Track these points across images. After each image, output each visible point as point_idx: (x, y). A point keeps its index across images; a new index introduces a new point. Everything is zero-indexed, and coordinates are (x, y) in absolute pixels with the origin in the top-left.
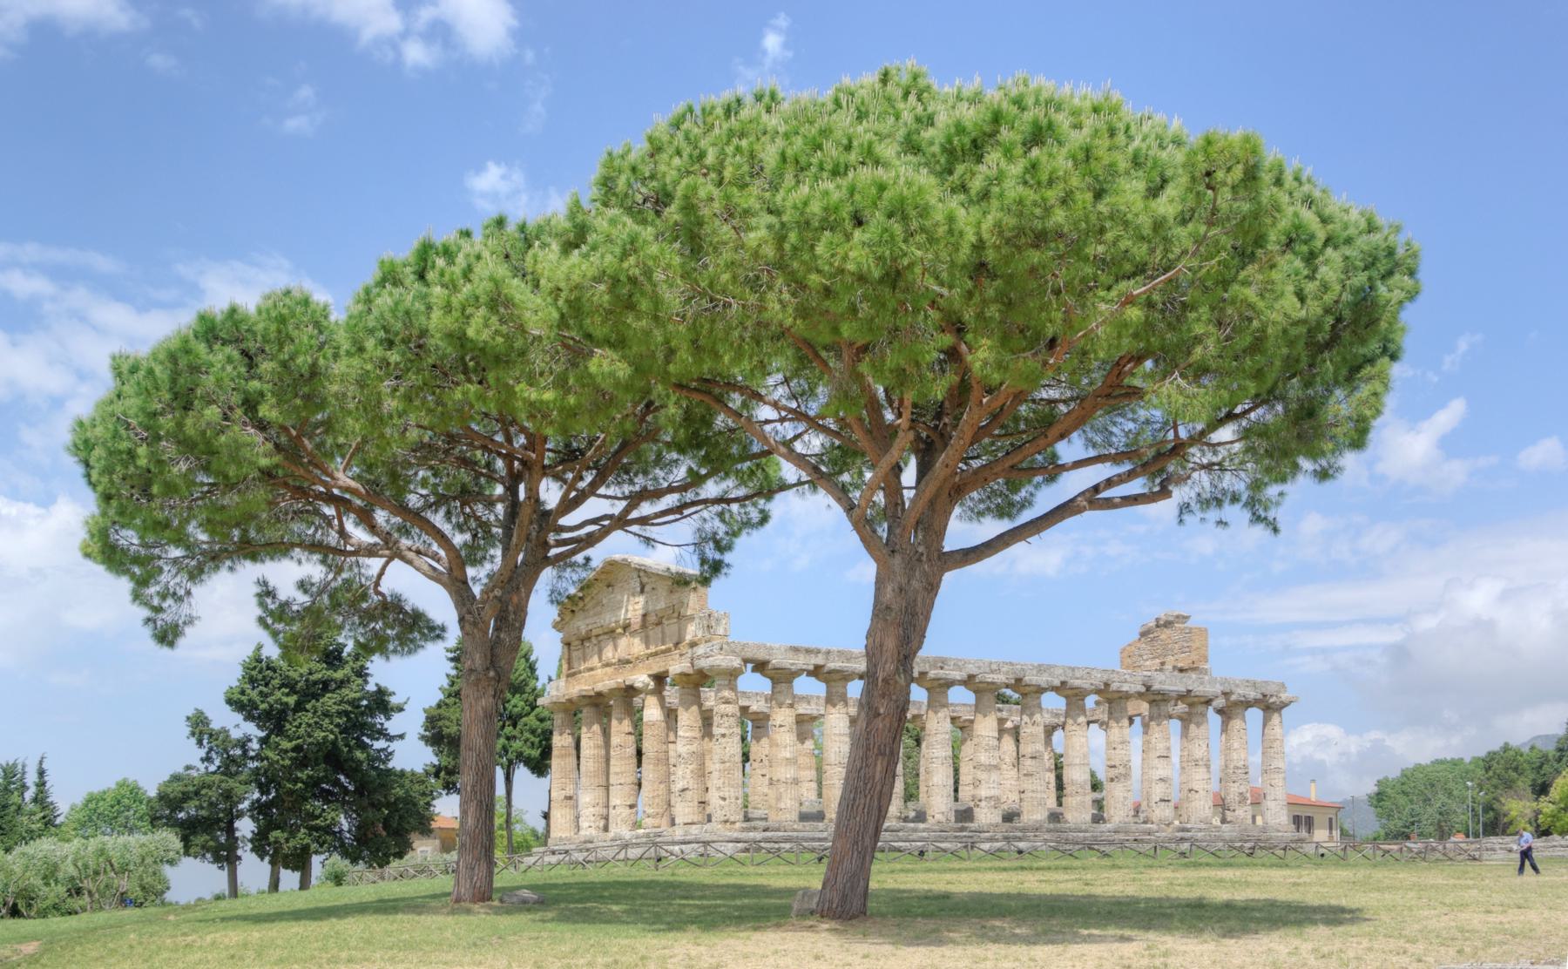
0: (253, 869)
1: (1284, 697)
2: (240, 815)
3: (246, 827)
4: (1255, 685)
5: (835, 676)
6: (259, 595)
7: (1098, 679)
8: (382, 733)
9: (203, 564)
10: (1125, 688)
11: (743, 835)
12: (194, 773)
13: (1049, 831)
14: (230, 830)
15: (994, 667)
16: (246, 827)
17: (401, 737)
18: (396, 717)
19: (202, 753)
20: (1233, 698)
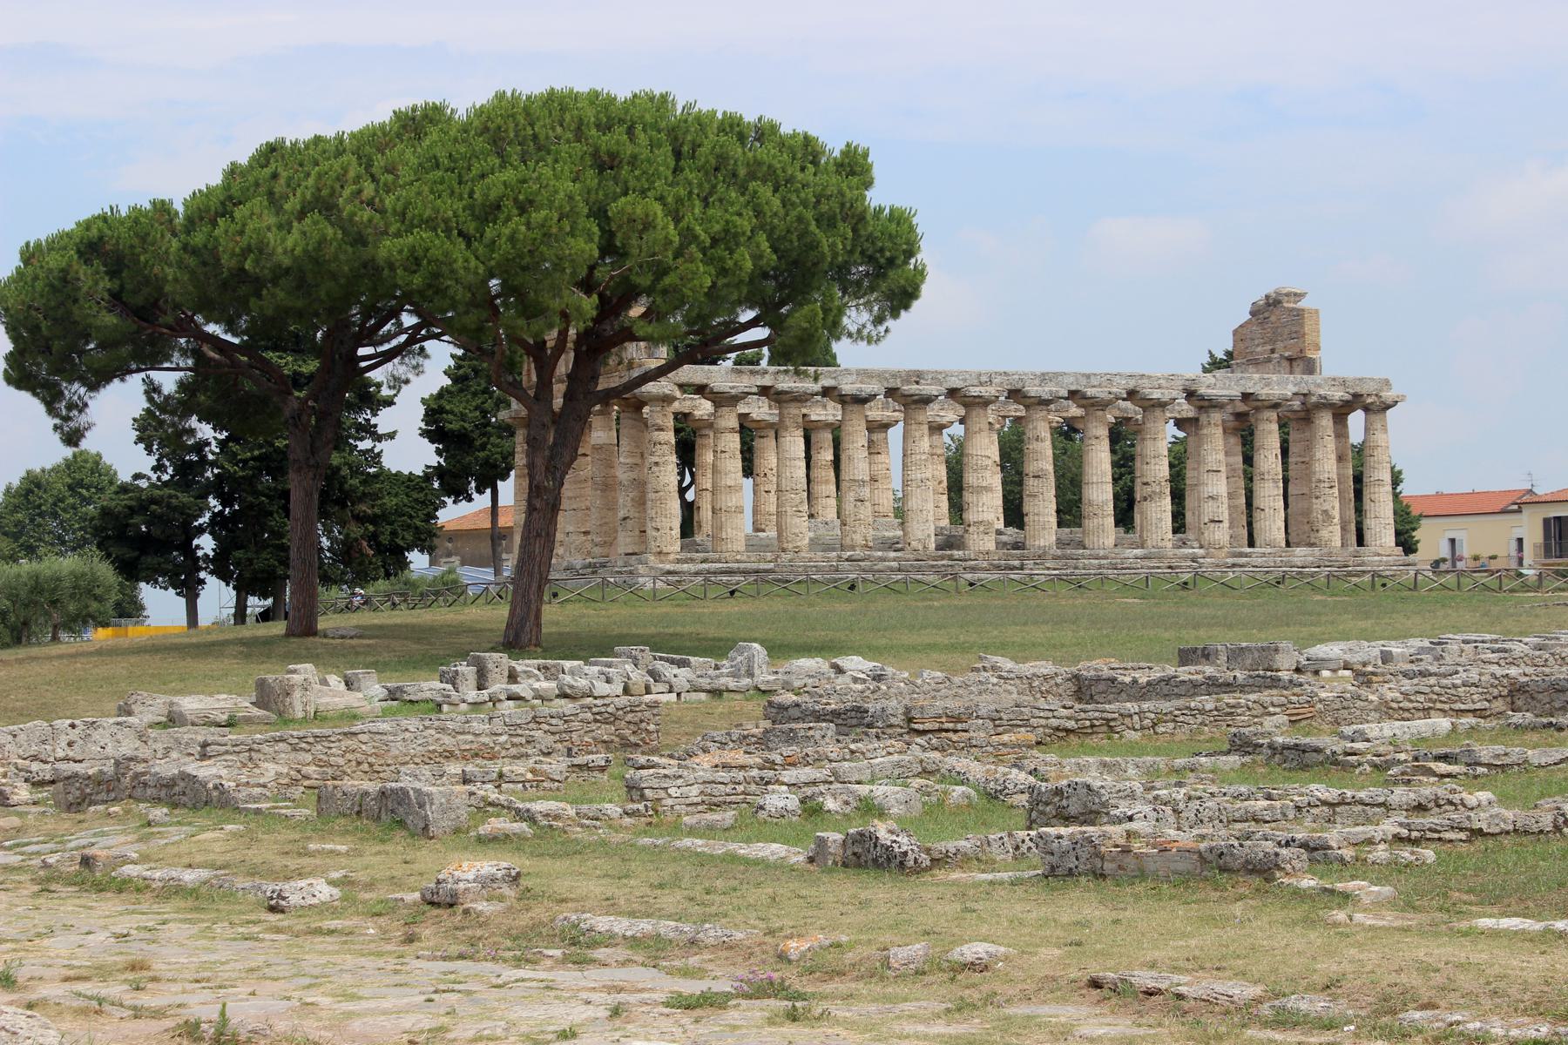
0: (217, 597)
1: (1388, 395)
2: (200, 530)
3: (206, 544)
4: (1344, 382)
5: (785, 397)
6: (146, 392)
7: (1119, 388)
8: (369, 430)
9: (98, 379)
10: (1156, 395)
11: (678, 567)
12: (143, 484)
13: (1055, 558)
14: (189, 551)
15: (984, 379)
16: (206, 544)
17: (391, 436)
18: (385, 413)
19: (152, 461)
20: (1314, 399)
